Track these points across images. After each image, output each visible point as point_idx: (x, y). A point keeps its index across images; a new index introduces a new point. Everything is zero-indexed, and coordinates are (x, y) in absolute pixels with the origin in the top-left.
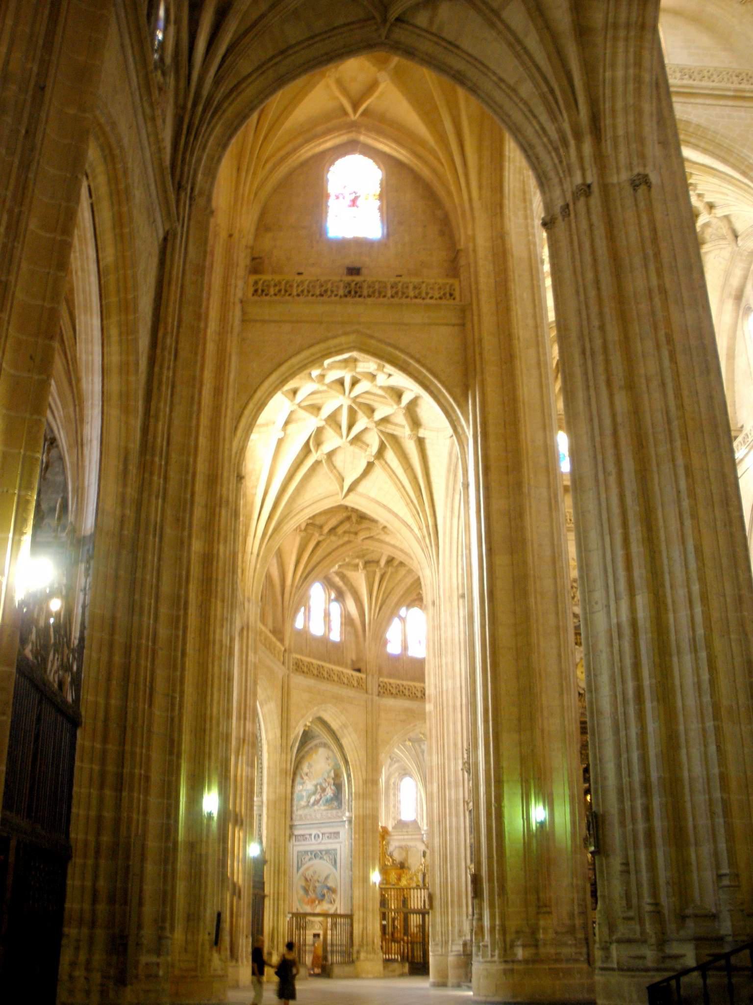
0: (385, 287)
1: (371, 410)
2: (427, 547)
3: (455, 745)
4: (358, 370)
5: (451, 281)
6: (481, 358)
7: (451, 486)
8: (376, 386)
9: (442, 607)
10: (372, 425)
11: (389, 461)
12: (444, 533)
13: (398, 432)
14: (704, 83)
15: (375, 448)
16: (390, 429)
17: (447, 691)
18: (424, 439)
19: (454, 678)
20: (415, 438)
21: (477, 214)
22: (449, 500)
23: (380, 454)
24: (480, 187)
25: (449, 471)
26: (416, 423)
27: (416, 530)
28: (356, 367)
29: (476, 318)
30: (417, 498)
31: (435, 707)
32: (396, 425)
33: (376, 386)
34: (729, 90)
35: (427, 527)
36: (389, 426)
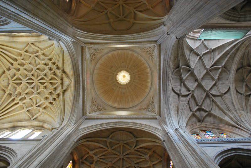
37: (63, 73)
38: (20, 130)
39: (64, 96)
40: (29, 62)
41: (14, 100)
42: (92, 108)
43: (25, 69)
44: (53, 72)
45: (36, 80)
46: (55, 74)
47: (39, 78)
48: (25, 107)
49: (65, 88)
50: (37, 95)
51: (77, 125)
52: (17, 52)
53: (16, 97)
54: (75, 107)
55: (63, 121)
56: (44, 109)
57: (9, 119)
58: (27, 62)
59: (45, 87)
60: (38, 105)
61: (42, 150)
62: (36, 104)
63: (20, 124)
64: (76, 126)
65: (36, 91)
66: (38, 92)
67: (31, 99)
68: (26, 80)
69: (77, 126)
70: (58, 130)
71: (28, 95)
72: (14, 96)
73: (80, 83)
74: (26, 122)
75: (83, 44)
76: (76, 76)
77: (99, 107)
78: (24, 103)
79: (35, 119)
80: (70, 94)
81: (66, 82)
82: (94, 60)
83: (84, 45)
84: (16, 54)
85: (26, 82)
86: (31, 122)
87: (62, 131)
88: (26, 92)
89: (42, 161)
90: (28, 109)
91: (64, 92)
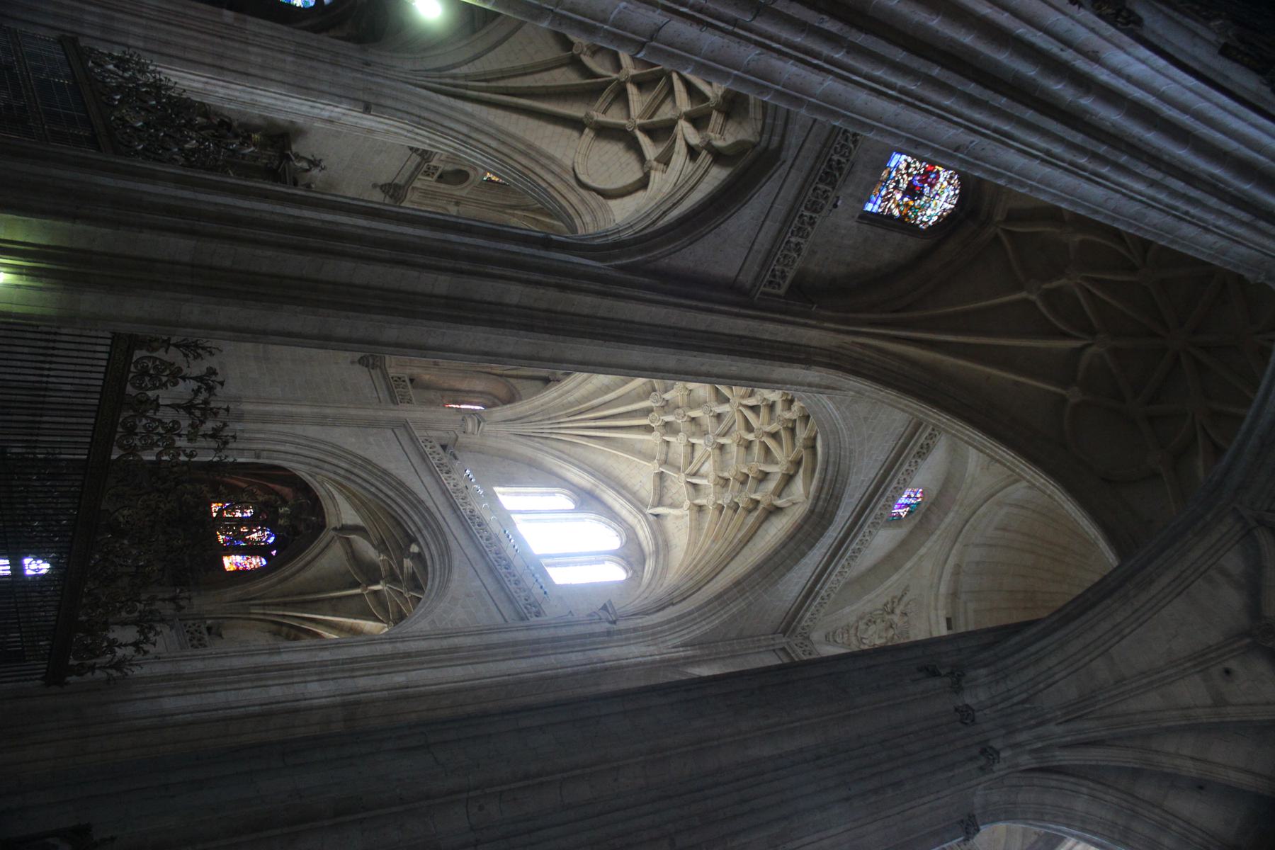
0: (815, 211)
1: (642, 84)
2: (440, 77)
3: (167, 43)
4: (715, 114)
5: (785, 285)
6: (690, 307)
7: (509, 140)
8: (679, 118)
9: (359, 75)
10: (622, 76)
11: (564, 69)
12: (452, 108)
13: (601, 102)
14: (839, 569)
15: (587, 60)
16: (607, 95)
17: (248, 52)
18: (581, 131)
19: (262, 67)
20: (585, 120)
21: (841, 336)
22: (493, 131)
23: (576, 63)
24: (863, 345)
25: (530, 146)
26: (605, 132)
27: (464, 70)
28: (719, 111)
29: (736, 310)
30: (507, 88)
31: (228, 26)
32: (610, 104)
33: (679, 118)
34: (821, 588)
35: (466, 87)
36: (612, 96)
37: (806, 447)
38: (593, 516)
39: (762, 523)
41: (647, 412)
42: (862, 626)
44: (790, 420)
45: (738, 401)
46: (792, 431)
48: (663, 457)
49: (779, 503)
50: (709, 449)
51: (690, 653)
53: (662, 407)
55: (673, 604)
56: (696, 509)
57: (600, 460)
59: (748, 445)
60: (694, 481)
61: (458, 658)
62: (695, 474)
63: (610, 497)
64: (682, 654)
65: (718, 435)
66: (722, 441)
67: (693, 445)
70: (614, 622)
71: (694, 428)
72: (657, 402)
73: (825, 528)
74: (628, 506)
76: (823, 496)
79: (657, 516)
80: (777, 529)
81: (798, 487)
86: (640, 517)
87: (606, 638)
88: (694, 414)
89: (411, 687)
91: (774, 511)
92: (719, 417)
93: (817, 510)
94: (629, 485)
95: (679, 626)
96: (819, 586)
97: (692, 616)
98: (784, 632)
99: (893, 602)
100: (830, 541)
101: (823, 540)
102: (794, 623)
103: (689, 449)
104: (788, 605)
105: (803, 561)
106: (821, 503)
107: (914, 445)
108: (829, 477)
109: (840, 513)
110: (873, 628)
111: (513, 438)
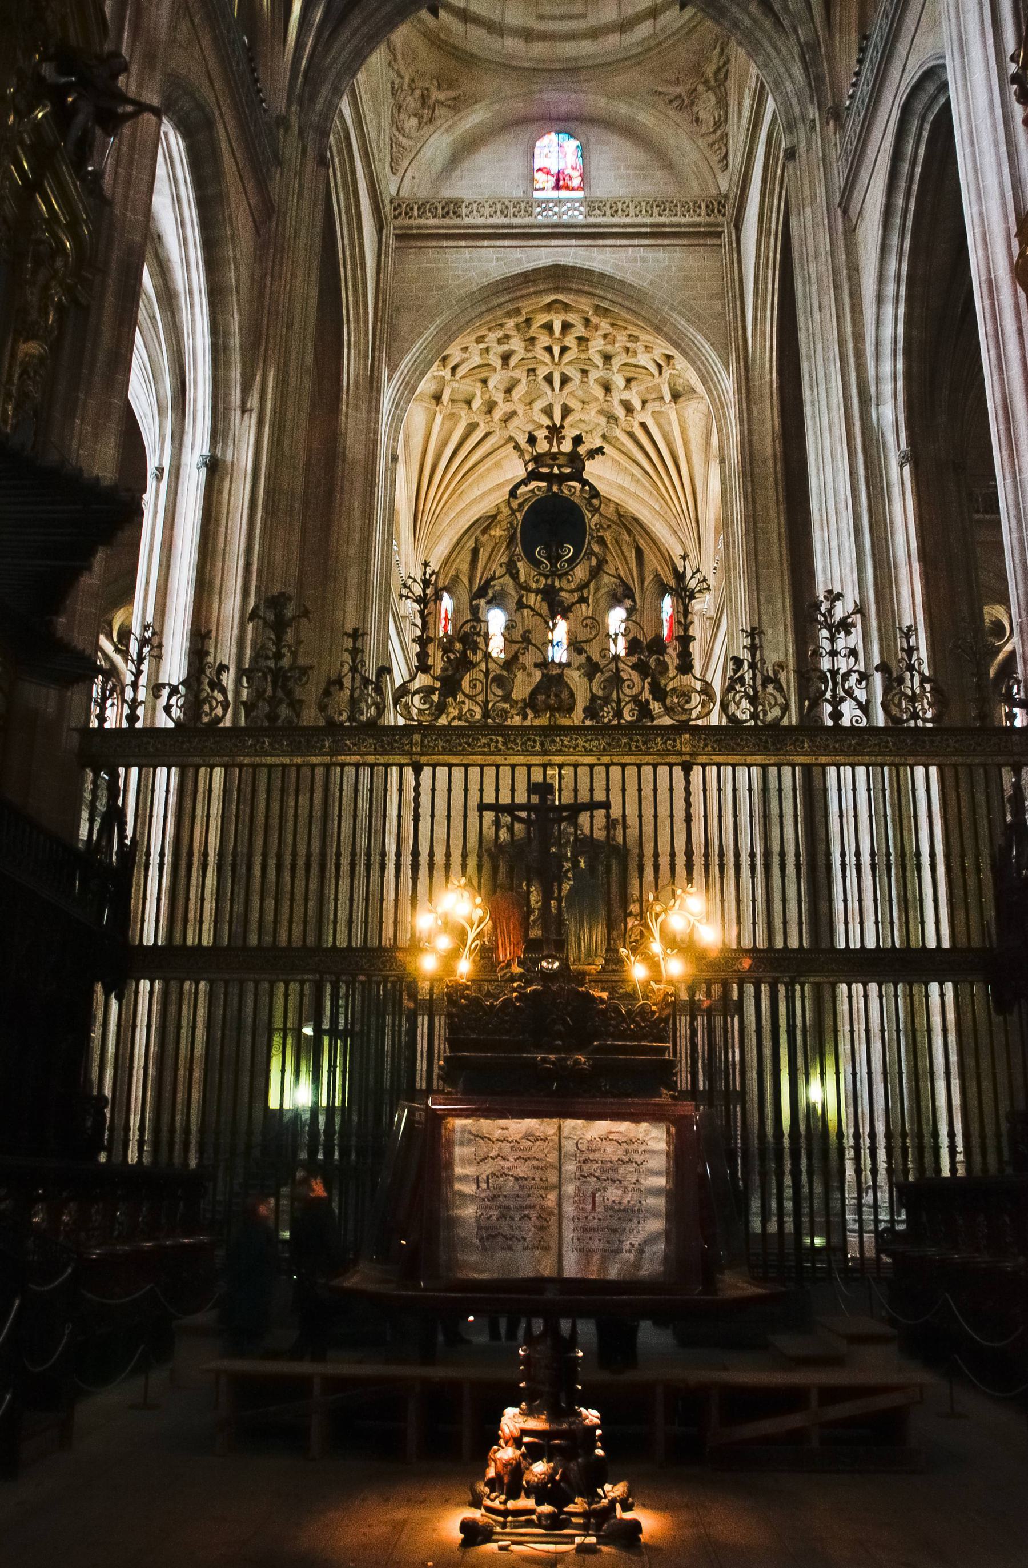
40: (479, 385)
42: (704, 129)
43: (509, 391)
47: (547, 358)
50: (615, 369)
52: (443, 424)
54: (664, 321)
56: (672, 362)
58: (478, 393)
67: (628, 381)
68: (553, 390)
69: (738, 362)
73: (564, 268)
75: (387, 245)
76: (532, 290)
77: (710, 70)
78: (644, 403)
82: (451, 86)
83: (390, 232)
84: (448, 424)
85: (561, 390)
90: (668, 397)
92: (585, 372)
93: (552, 286)
94: (703, 424)
95: (712, 380)
96: (643, 230)
97: (701, 366)
98: (719, 235)
99: (671, 102)
100: (581, 251)
101: (580, 263)
102: (702, 230)
103: (633, 384)
104: (678, 254)
105: (609, 270)
106: (541, 287)
107: (443, 227)
108: (507, 298)
109: (540, 264)
110: (702, 115)
111: (703, 556)
